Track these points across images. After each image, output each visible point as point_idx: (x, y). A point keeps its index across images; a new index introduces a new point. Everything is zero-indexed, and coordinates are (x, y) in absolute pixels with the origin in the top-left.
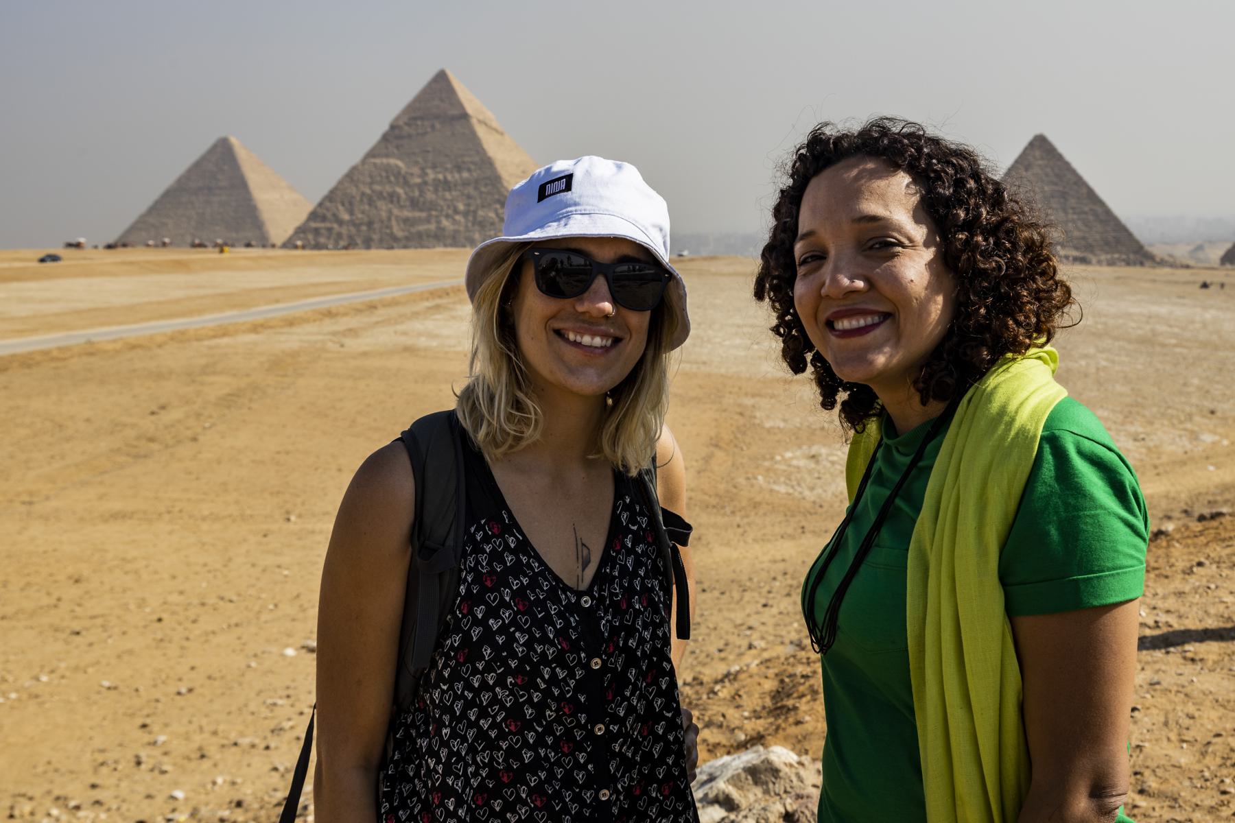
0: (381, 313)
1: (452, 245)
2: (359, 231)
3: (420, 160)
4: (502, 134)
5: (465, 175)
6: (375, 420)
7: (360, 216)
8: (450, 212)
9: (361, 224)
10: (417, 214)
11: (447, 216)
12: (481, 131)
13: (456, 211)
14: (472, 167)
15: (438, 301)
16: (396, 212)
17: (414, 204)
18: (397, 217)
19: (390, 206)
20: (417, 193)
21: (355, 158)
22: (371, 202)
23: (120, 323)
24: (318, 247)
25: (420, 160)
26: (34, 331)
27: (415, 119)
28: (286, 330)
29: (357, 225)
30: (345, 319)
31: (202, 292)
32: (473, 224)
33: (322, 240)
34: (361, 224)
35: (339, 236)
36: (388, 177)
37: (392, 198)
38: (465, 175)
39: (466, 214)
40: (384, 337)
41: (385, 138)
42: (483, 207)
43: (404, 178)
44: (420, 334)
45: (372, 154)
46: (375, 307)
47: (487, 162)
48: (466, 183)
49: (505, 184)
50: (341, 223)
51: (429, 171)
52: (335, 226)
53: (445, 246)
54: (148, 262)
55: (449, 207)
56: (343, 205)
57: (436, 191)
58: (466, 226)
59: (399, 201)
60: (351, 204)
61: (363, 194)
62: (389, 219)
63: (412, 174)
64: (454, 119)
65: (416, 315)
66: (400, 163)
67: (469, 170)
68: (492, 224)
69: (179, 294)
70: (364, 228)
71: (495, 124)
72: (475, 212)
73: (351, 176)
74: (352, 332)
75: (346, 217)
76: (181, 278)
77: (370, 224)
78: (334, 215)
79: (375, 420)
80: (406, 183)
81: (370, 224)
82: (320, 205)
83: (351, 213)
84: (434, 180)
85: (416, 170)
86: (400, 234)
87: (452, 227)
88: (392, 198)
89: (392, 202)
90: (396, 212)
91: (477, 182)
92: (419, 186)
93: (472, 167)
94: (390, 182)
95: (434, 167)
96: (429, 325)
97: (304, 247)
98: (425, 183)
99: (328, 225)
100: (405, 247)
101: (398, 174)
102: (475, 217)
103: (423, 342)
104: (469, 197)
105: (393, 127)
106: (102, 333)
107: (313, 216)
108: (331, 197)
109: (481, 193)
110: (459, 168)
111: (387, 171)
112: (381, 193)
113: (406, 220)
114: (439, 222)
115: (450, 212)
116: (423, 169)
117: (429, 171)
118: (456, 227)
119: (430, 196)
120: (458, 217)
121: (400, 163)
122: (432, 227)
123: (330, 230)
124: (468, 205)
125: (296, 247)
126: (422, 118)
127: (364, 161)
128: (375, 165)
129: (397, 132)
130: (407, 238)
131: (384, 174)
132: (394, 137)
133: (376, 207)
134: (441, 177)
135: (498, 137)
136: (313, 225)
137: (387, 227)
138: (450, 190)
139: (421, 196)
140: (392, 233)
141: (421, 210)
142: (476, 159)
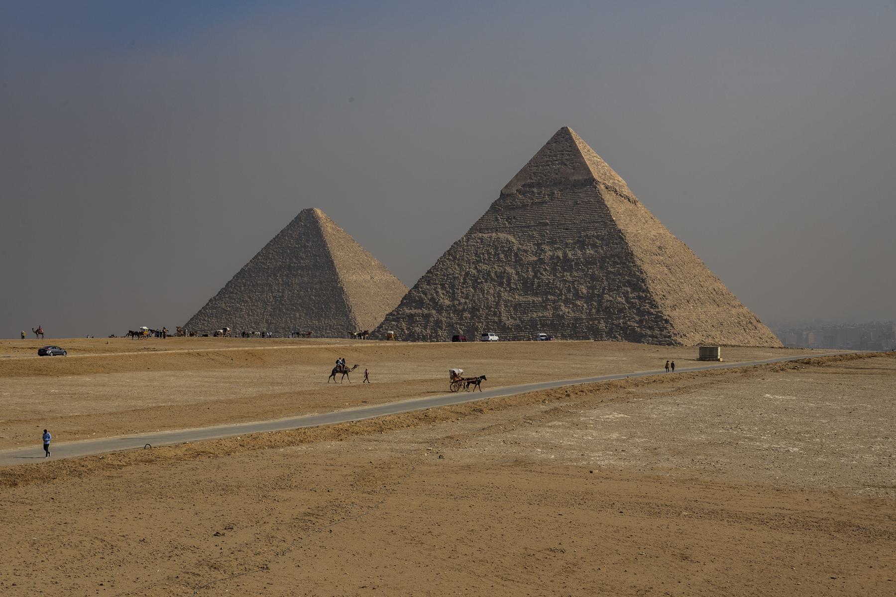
0: (488, 418)
1: (571, 338)
2: (461, 319)
3: (536, 234)
4: (635, 202)
5: (590, 251)
6: (480, 550)
7: (463, 301)
8: (570, 296)
9: (464, 310)
10: (530, 298)
11: (567, 301)
12: (609, 199)
13: (577, 296)
14: (599, 242)
15: (556, 404)
16: (505, 295)
17: (527, 287)
18: (506, 301)
19: (498, 288)
20: (531, 274)
21: (460, 233)
22: (476, 284)
23: (185, 426)
24: (412, 337)
25: (536, 234)
26: (88, 432)
27: (531, 185)
28: (372, 437)
29: (459, 313)
30: (444, 424)
31: (277, 389)
32: (598, 311)
33: (418, 329)
34: (464, 310)
35: (438, 324)
36: (497, 254)
37: (501, 279)
38: (590, 251)
39: (589, 299)
40: (492, 447)
41: (494, 208)
42: (610, 290)
43: (516, 255)
44: (535, 444)
45: (478, 227)
46: (481, 411)
47: (618, 236)
48: (589, 262)
49: (638, 263)
50: (440, 309)
51: (547, 248)
52: (434, 312)
53: (564, 337)
54: (217, 353)
55: (569, 290)
56: (443, 287)
57: (554, 270)
58: (590, 314)
59: (509, 284)
60: (453, 286)
61: (467, 274)
62: (497, 304)
63: (526, 251)
64: (576, 185)
65: (529, 421)
66: (511, 238)
67: (594, 246)
68: (621, 310)
69: (251, 391)
70: (467, 315)
71: (626, 191)
72: (601, 296)
73: (451, 253)
74: (452, 440)
75: (447, 302)
76: (255, 373)
77: (474, 310)
78: (433, 299)
79: (480, 550)
80: (519, 261)
81: (474, 310)
82: (416, 287)
83: (453, 297)
84: (552, 258)
85: (530, 246)
86: (509, 323)
87: (572, 315)
88: (501, 279)
89: (501, 284)
90: (505, 295)
91: (603, 260)
92: (534, 264)
93: (599, 242)
94: (499, 260)
95: (552, 243)
96: (546, 433)
97: (396, 339)
98: (541, 261)
99: (426, 312)
100: (515, 338)
101: (508, 252)
102: (600, 303)
103: (539, 453)
104: (593, 278)
105: (503, 195)
106: (164, 436)
107: (408, 300)
108: (428, 278)
109: (608, 273)
110: (582, 245)
111: (496, 248)
112: (489, 274)
113: (517, 306)
114: (556, 309)
115: (570, 296)
116: (539, 245)
117: (547, 248)
118: (577, 314)
119: (546, 277)
120: (578, 303)
121: (511, 238)
122: (549, 314)
123: (427, 317)
124: (593, 288)
125: (389, 338)
126: (539, 185)
127: (468, 236)
128: (481, 239)
129: (508, 201)
130: (518, 328)
131: (492, 251)
132: (505, 206)
133: (482, 291)
134: (560, 254)
135: (632, 207)
136: (408, 311)
137: (495, 314)
138: (570, 269)
139: (535, 276)
140: (500, 321)
141: (536, 294)
142: (604, 232)
